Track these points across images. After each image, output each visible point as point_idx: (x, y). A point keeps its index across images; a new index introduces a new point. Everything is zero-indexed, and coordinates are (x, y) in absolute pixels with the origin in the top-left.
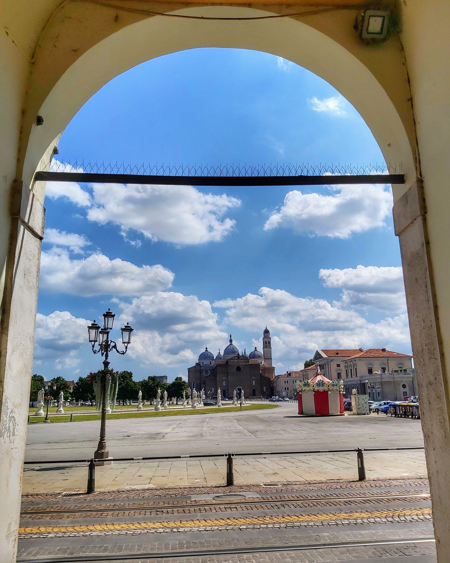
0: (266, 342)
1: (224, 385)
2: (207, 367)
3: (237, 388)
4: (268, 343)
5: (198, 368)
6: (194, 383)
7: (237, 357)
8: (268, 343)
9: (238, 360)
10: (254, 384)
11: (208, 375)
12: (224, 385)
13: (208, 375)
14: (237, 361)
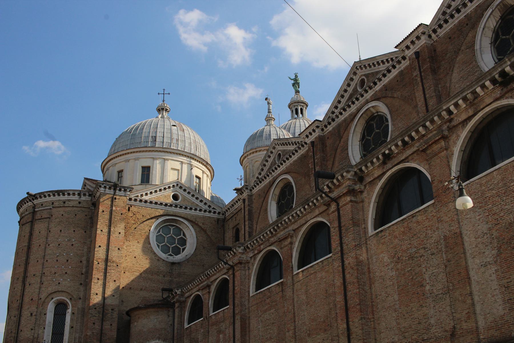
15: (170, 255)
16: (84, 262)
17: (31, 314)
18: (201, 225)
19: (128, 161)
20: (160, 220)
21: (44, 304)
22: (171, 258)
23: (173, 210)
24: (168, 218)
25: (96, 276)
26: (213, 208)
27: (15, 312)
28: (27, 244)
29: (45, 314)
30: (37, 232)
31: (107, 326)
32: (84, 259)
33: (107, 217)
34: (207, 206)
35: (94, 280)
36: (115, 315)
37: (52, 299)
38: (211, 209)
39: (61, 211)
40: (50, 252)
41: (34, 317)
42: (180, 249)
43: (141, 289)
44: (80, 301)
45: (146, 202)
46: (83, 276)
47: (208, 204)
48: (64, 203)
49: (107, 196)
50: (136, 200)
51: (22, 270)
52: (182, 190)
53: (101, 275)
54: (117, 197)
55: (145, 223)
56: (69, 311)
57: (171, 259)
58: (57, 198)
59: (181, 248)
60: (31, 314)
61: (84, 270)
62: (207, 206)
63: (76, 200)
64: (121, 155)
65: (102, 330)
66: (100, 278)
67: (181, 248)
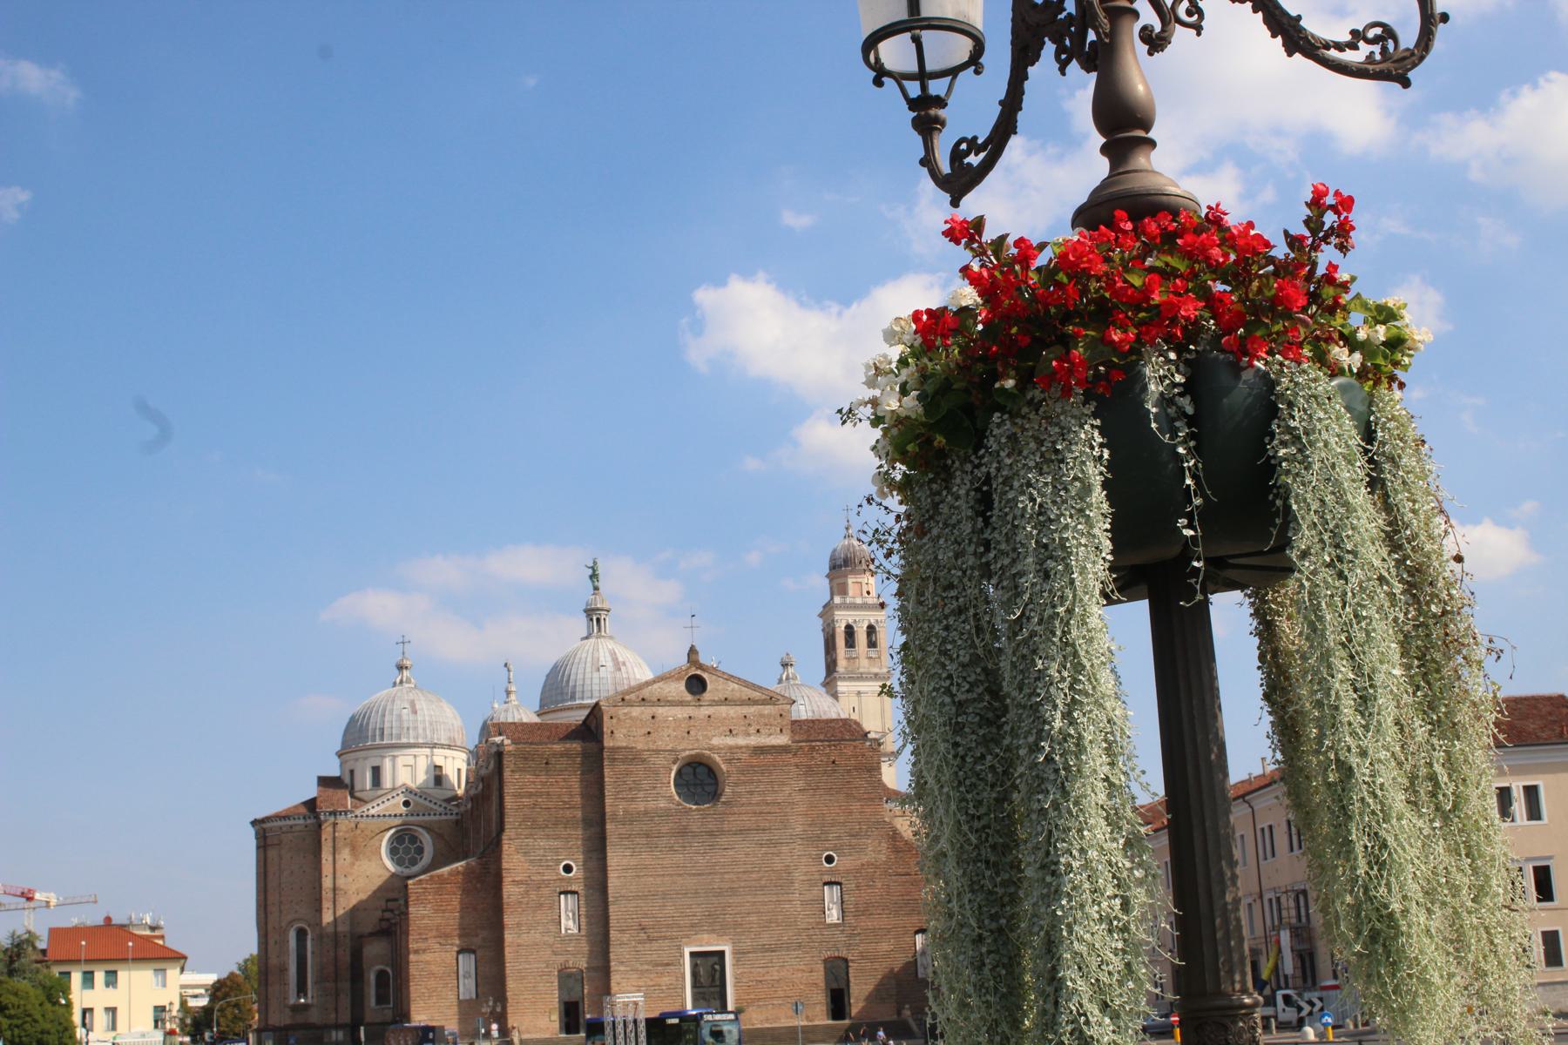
0: (850, 631)
2: (406, 804)
3: (687, 951)
4: (861, 637)
6: (301, 934)
7: (682, 686)
8: (861, 637)
10: (833, 916)
12: (569, 924)
14: (680, 713)
15: (407, 867)
19: (357, 760)
35: (324, 910)
36: (348, 941)
39: (290, 836)
45: (373, 816)
49: (328, 823)
51: (262, 897)
56: (309, 937)
57: (407, 872)
62: (442, 809)
65: (336, 957)
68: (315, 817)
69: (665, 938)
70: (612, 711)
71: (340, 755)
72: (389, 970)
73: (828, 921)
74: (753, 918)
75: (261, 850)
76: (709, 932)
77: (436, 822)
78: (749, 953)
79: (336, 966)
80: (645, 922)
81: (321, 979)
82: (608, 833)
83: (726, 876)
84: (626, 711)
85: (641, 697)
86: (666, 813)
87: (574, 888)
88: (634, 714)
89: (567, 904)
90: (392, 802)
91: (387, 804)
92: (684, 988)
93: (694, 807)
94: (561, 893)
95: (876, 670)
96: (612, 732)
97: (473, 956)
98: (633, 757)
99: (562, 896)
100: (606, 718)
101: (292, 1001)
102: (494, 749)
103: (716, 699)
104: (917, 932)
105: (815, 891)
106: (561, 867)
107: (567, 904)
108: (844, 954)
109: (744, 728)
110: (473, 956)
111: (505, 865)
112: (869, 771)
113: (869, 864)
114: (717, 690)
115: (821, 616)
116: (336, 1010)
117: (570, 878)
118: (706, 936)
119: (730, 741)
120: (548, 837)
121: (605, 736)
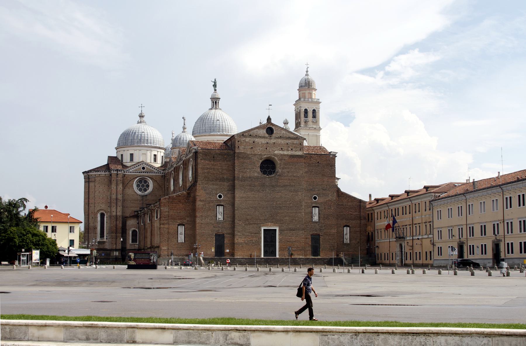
0: (306, 111)
1: (220, 217)
2: (143, 168)
3: (263, 229)
4: (310, 114)
5: (117, 170)
6: (102, 215)
7: (265, 131)
8: (310, 114)
9: (267, 140)
10: (316, 218)
11: (146, 193)
12: (220, 217)
13: (146, 193)
14: (264, 141)
16: (109, 198)
17: (92, 218)
18: (155, 179)
20: (138, 179)
21: (96, 214)
22: (143, 193)
23: (142, 174)
24: (141, 177)
25: (113, 205)
26: (160, 171)
27: (87, 217)
28: (88, 191)
29: (97, 218)
30: (91, 186)
31: (118, 222)
32: (109, 197)
33: (116, 182)
34: (157, 171)
36: (121, 219)
37: (99, 212)
38: (159, 172)
39: (99, 178)
40: (96, 194)
41: (93, 219)
42: (147, 189)
43: (131, 207)
44: (109, 213)
45: (131, 172)
46: (109, 203)
47: (157, 170)
48: (100, 175)
50: (127, 172)
51: (87, 201)
52: (146, 165)
53: (115, 205)
54: (119, 174)
55: (131, 181)
56: (105, 216)
58: (96, 173)
59: (147, 189)
60: (92, 218)
61: (109, 201)
62: (157, 171)
63: (104, 174)
64: (121, 148)
65: (116, 224)
66: (114, 206)
67: (147, 189)
68: (109, 172)
69: (255, 224)
70: (239, 139)
71: (116, 149)
72: (137, 230)
73: (313, 220)
74: (287, 218)
75: (87, 183)
76: (270, 222)
77: (154, 176)
78: (285, 230)
79: (116, 228)
80: (248, 217)
81: (110, 232)
82: (236, 184)
83: (278, 202)
84: (244, 139)
85: (249, 134)
86: (257, 178)
87: (222, 204)
88: (247, 141)
89: (220, 209)
90: (138, 167)
91: (136, 168)
92: (261, 242)
93: (267, 176)
94: (217, 205)
95: (314, 126)
96: (238, 147)
97: (184, 227)
98: (246, 156)
99: (218, 207)
100: (236, 142)
101: (99, 239)
102: (194, 151)
103: (277, 136)
104: (344, 226)
105: (310, 209)
106: (218, 196)
107: (220, 209)
108: (318, 232)
109: (286, 148)
110: (183, 227)
111: (197, 194)
112: (331, 166)
113: (329, 200)
114: (278, 133)
115: (294, 105)
116: (116, 244)
117: (221, 200)
118: (270, 224)
119: (281, 152)
120: (213, 184)
121: (236, 148)
